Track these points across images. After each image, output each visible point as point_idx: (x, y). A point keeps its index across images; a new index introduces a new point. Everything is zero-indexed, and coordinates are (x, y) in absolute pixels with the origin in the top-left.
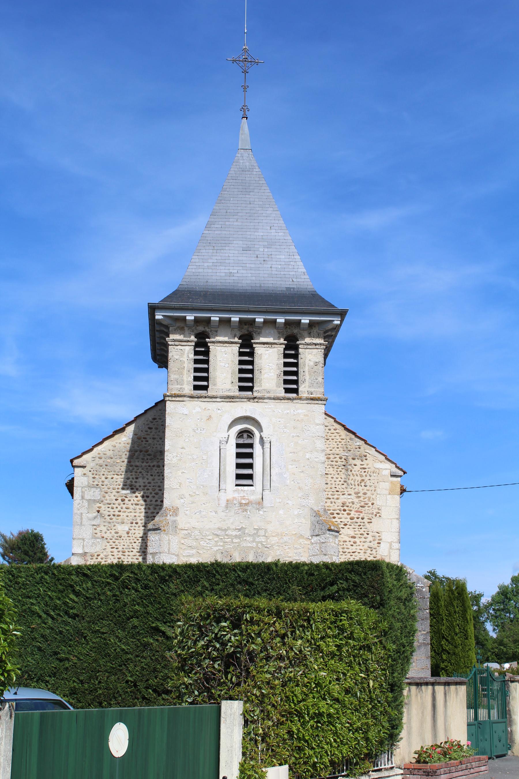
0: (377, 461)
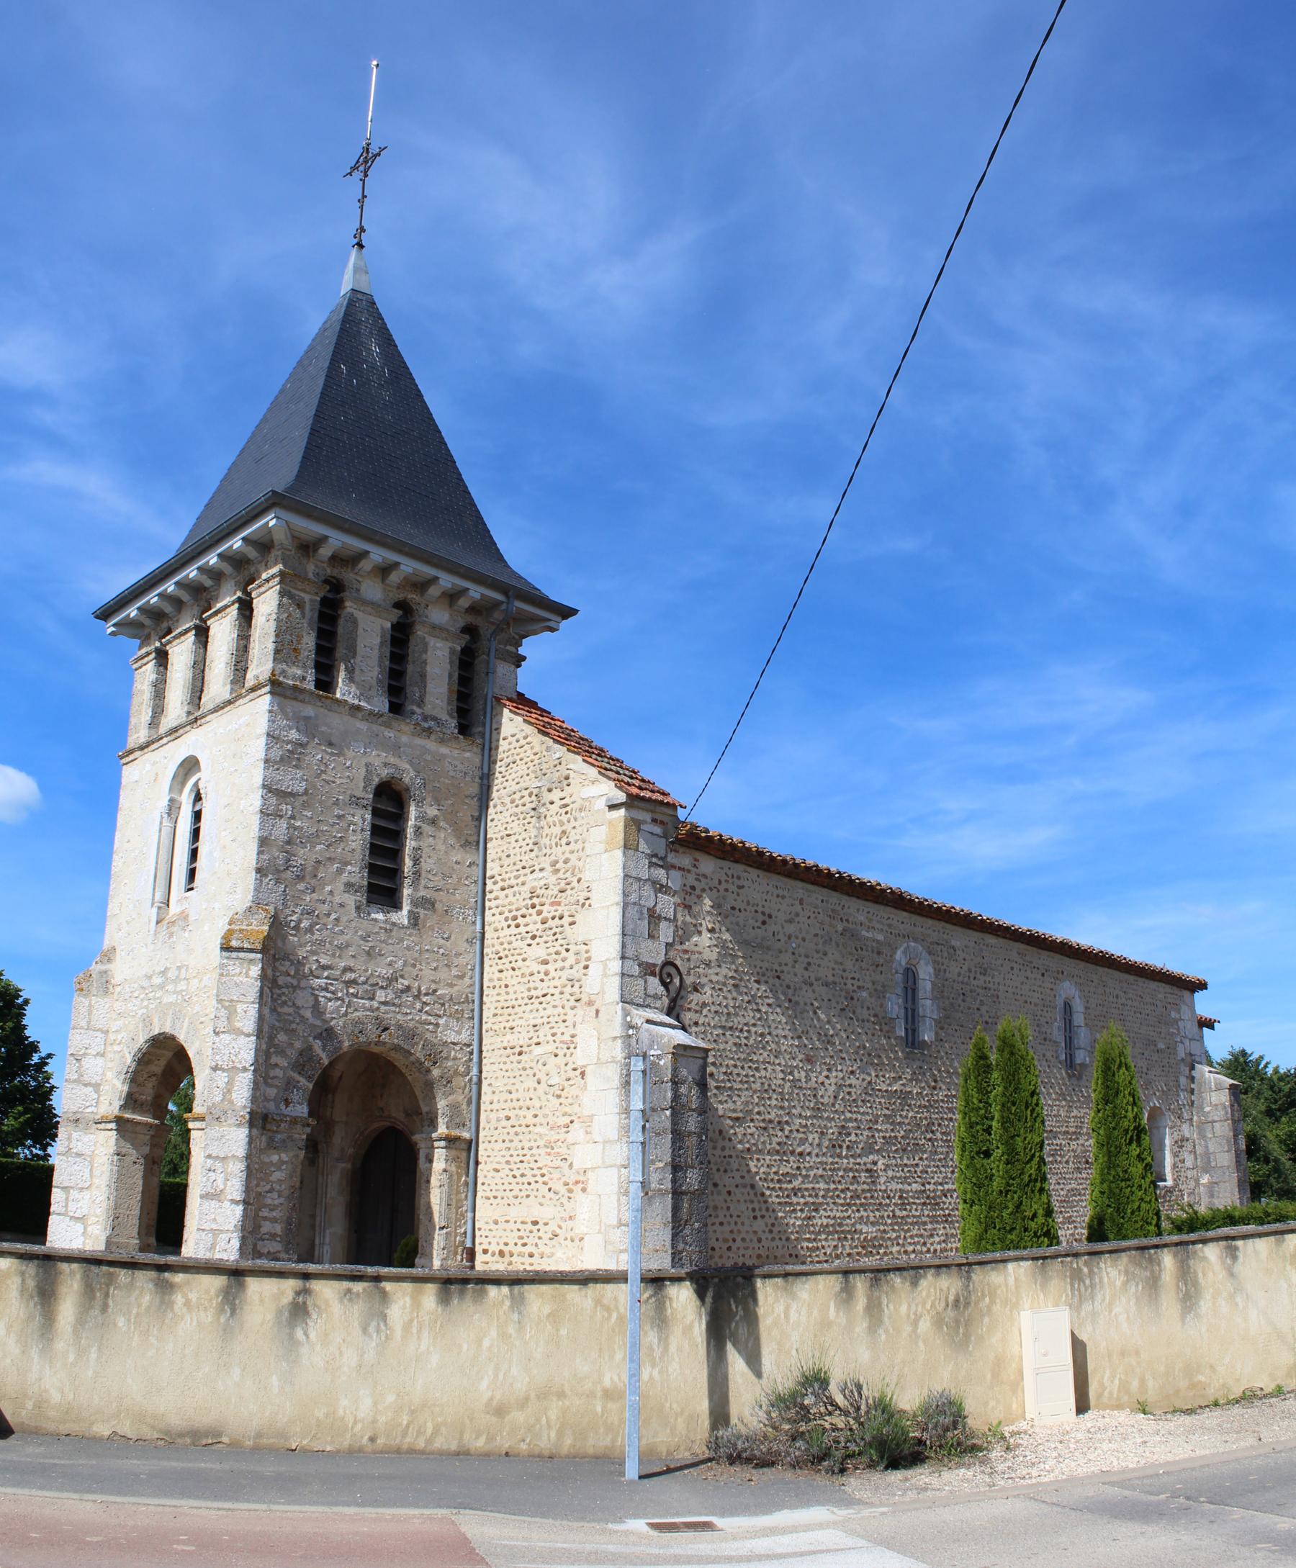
0: (586, 782)
